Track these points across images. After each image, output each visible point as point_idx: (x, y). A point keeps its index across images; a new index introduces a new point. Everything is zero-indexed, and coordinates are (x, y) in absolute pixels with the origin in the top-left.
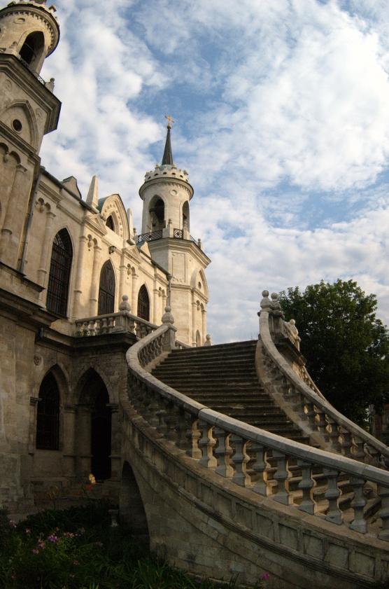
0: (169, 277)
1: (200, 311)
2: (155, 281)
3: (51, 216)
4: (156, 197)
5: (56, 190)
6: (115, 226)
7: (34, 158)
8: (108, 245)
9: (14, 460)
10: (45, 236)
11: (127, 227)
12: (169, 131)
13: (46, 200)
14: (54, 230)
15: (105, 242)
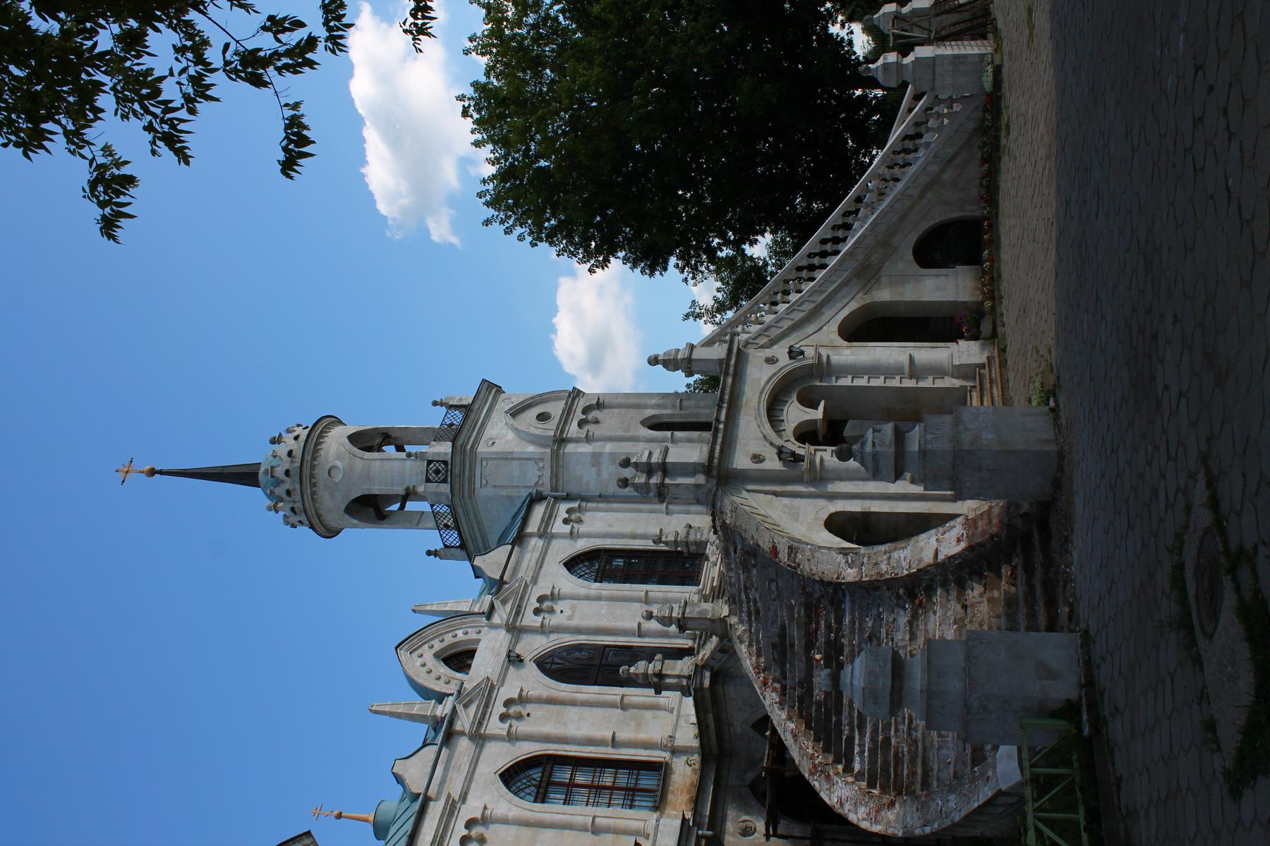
0: (535, 499)
2: (553, 536)
3: (488, 812)
5: (435, 811)
6: (460, 649)
8: (507, 669)
10: (528, 824)
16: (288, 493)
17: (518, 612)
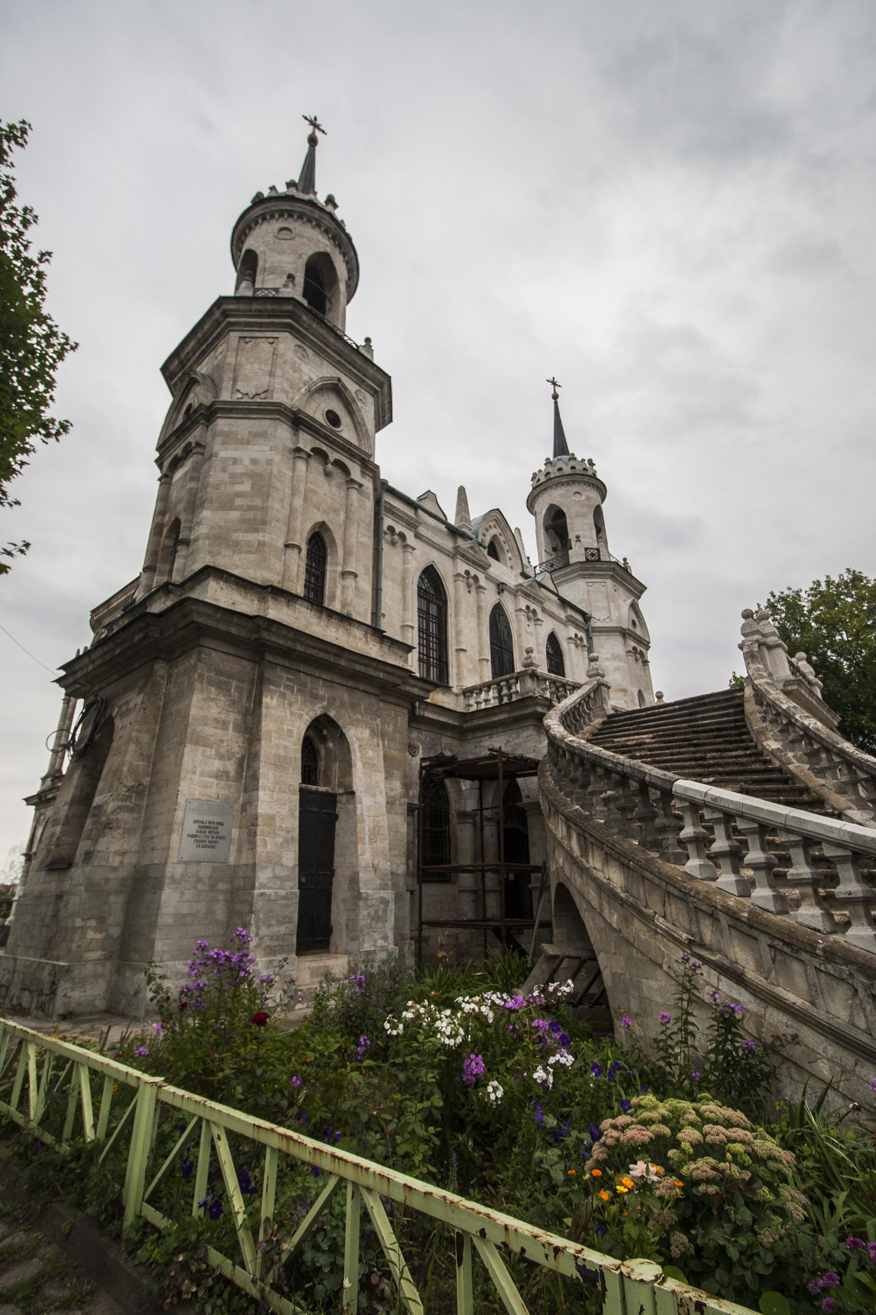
0: (587, 618)
1: (640, 661)
4: (552, 507)
5: (410, 512)
7: (370, 468)
9: (384, 901)
10: (404, 579)
11: (517, 554)
12: (556, 403)
13: (399, 528)
14: (415, 566)
15: (489, 578)
16: (560, 469)
17: (527, 595)
